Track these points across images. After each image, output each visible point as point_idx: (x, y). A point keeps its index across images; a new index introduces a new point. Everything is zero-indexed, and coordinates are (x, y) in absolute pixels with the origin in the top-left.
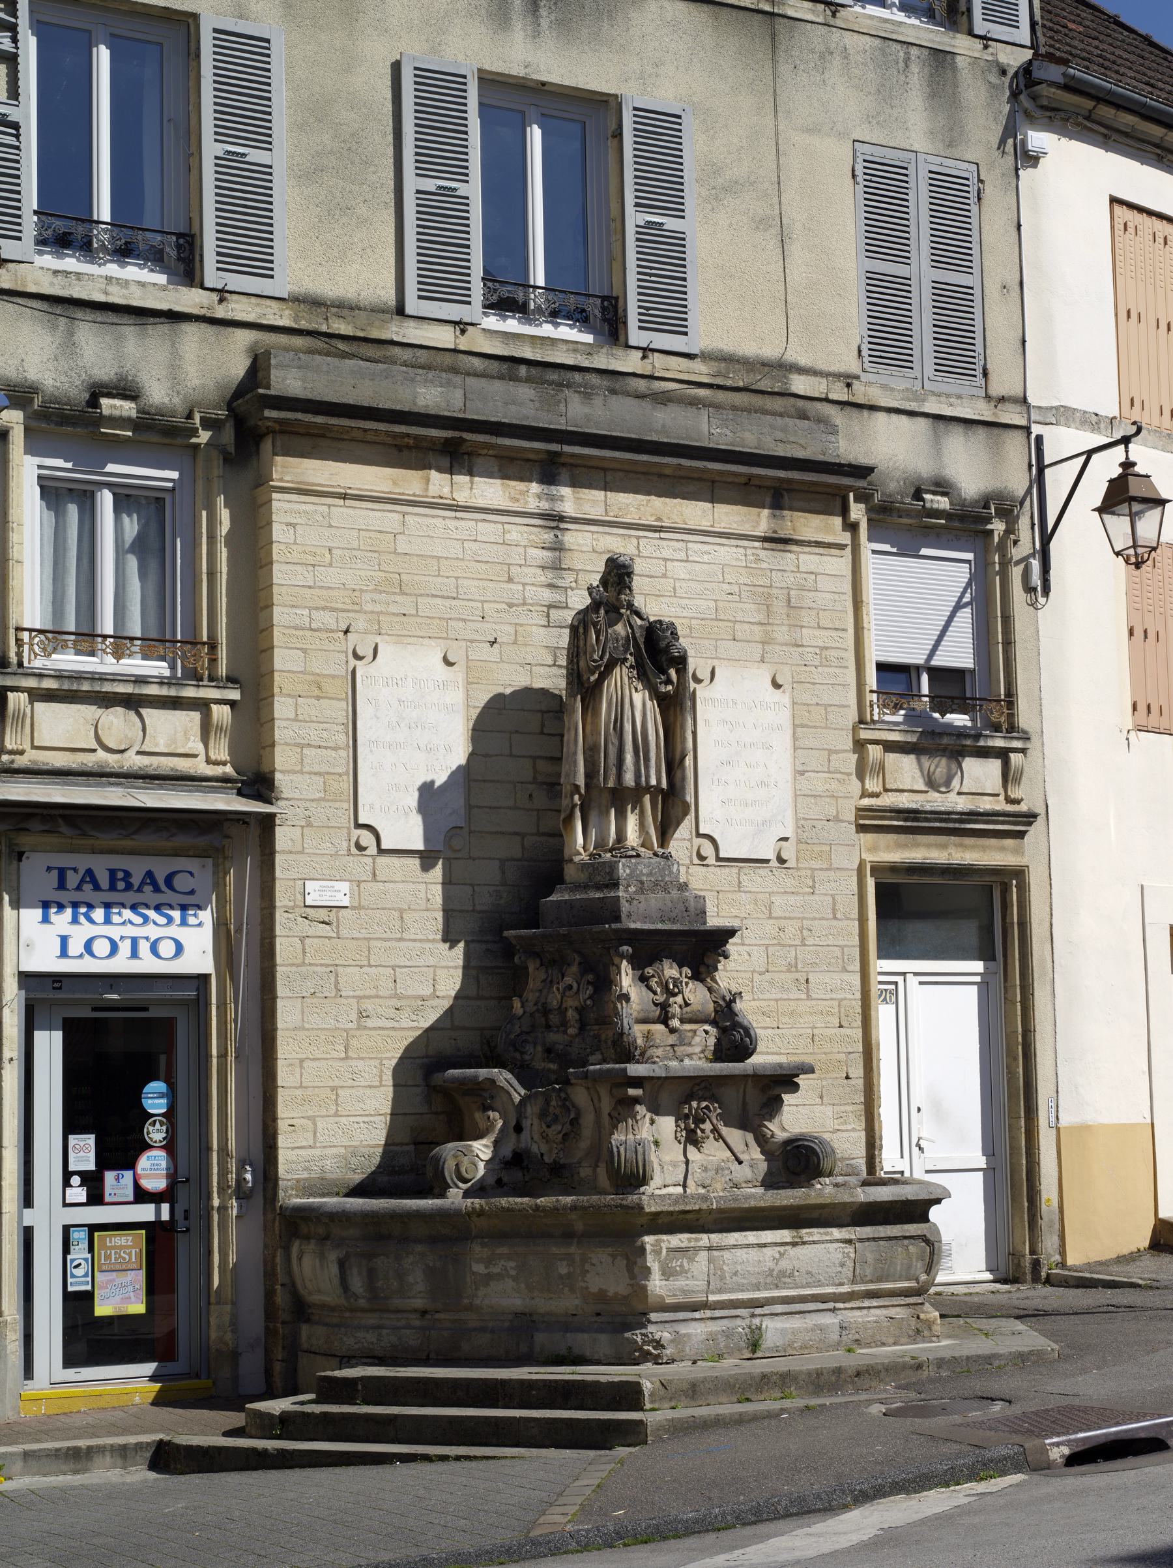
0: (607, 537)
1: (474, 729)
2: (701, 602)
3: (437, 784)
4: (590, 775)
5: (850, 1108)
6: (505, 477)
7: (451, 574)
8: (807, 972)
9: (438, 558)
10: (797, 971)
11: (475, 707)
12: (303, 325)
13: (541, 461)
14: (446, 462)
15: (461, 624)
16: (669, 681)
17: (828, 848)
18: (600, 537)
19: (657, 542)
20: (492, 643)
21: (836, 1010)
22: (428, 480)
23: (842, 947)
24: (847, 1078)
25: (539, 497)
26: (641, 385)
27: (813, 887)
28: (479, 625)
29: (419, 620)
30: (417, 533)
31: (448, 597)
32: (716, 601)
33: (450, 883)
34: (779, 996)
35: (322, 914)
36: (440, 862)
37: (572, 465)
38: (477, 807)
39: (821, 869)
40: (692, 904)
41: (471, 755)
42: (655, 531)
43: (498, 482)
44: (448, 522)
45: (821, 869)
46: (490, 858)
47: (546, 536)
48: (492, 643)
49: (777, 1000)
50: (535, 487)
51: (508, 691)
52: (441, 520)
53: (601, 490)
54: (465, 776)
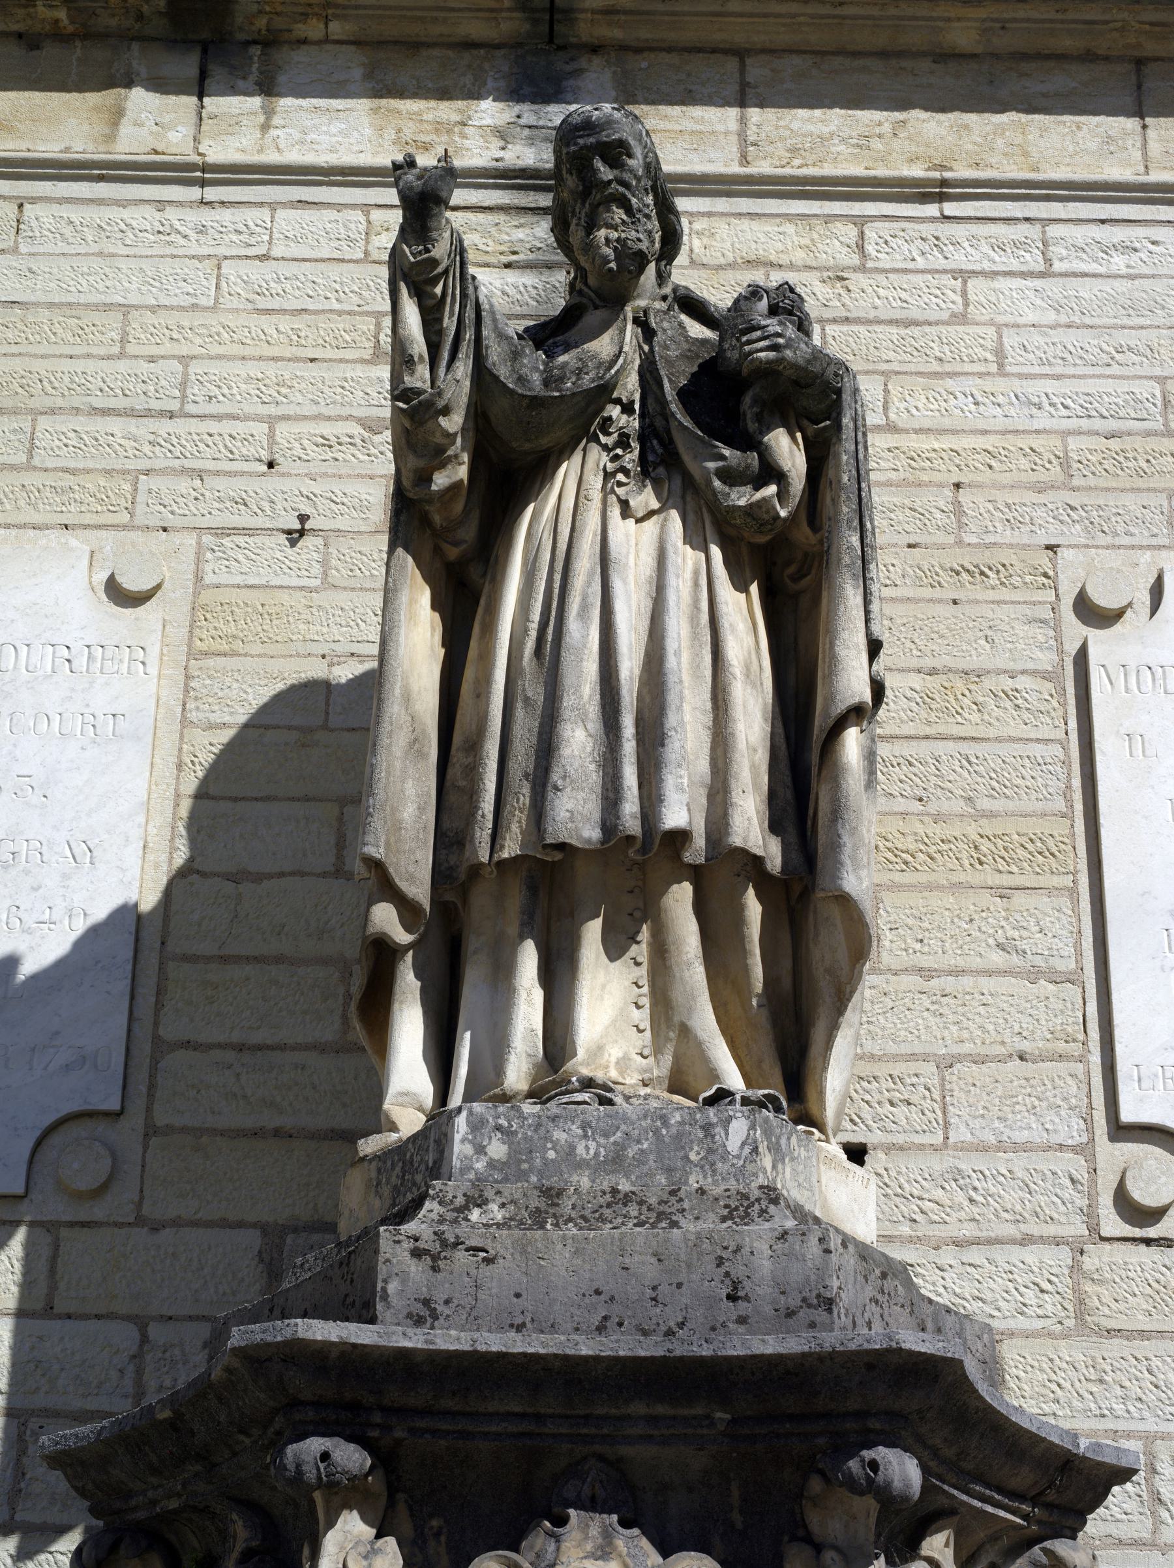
0: (745, 224)
1: (201, 795)
2: (1108, 386)
3: (27, 968)
4: (450, 835)
6: (382, 88)
7: (168, 348)
9: (126, 309)
11: (211, 726)
13: (514, 45)
14: (189, 66)
15: (184, 485)
16: (771, 472)
18: (721, 225)
19: (928, 229)
20: (295, 536)
22: (117, 114)
25: (503, 135)
28: (254, 485)
29: (30, 479)
30: (62, 247)
31: (148, 414)
32: (1162, 380)
33: (49, 1311)
36: (21, 1235)
37: (623, 48)
38: (187, 1045)
40: (764, 1265)
41: (181, 876)
42: (924, 198)
43: (362, 105)
44: (171, 214)
46: (224, 1224)
47: (520, 234)
48: (295, 536)
50: (490, 112)
51: (344, 673)
52: (149, 211)
53: (726, 103)
54: (135, 944)
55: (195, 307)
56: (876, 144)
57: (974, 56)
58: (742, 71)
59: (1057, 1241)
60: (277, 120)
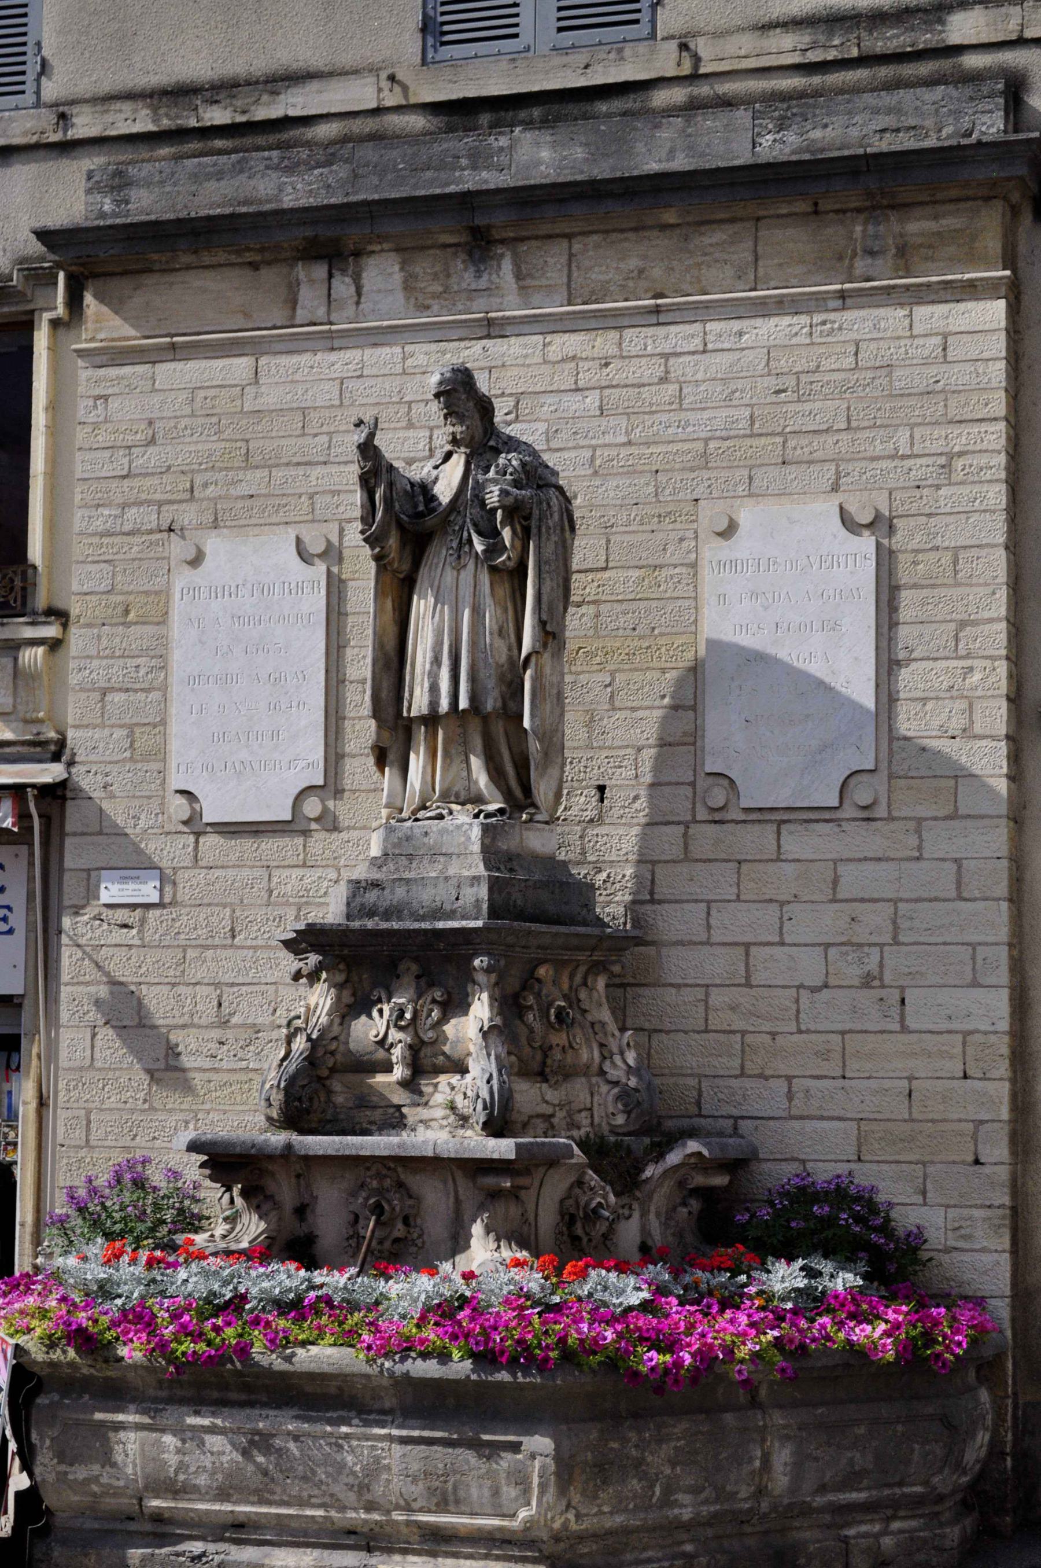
5: (977, 1213)
8: (902, 988)
10: (883, 986)
12: (166, 123)
17: (952, 782)
21: (959, 1049)
23: (974, 946)
24: (977, 1162)
26: (677, 95)
27: (920, 848)
34: (848, 1026)
35: (121, 916)
39: (935, 819)
45: (935, 819)
49: (843, 1033)
55: (333, 406)
56: (631, 284)
57: (678, 225)
58: (570, 248)
59: (679, 823)
60: (363, 300)
